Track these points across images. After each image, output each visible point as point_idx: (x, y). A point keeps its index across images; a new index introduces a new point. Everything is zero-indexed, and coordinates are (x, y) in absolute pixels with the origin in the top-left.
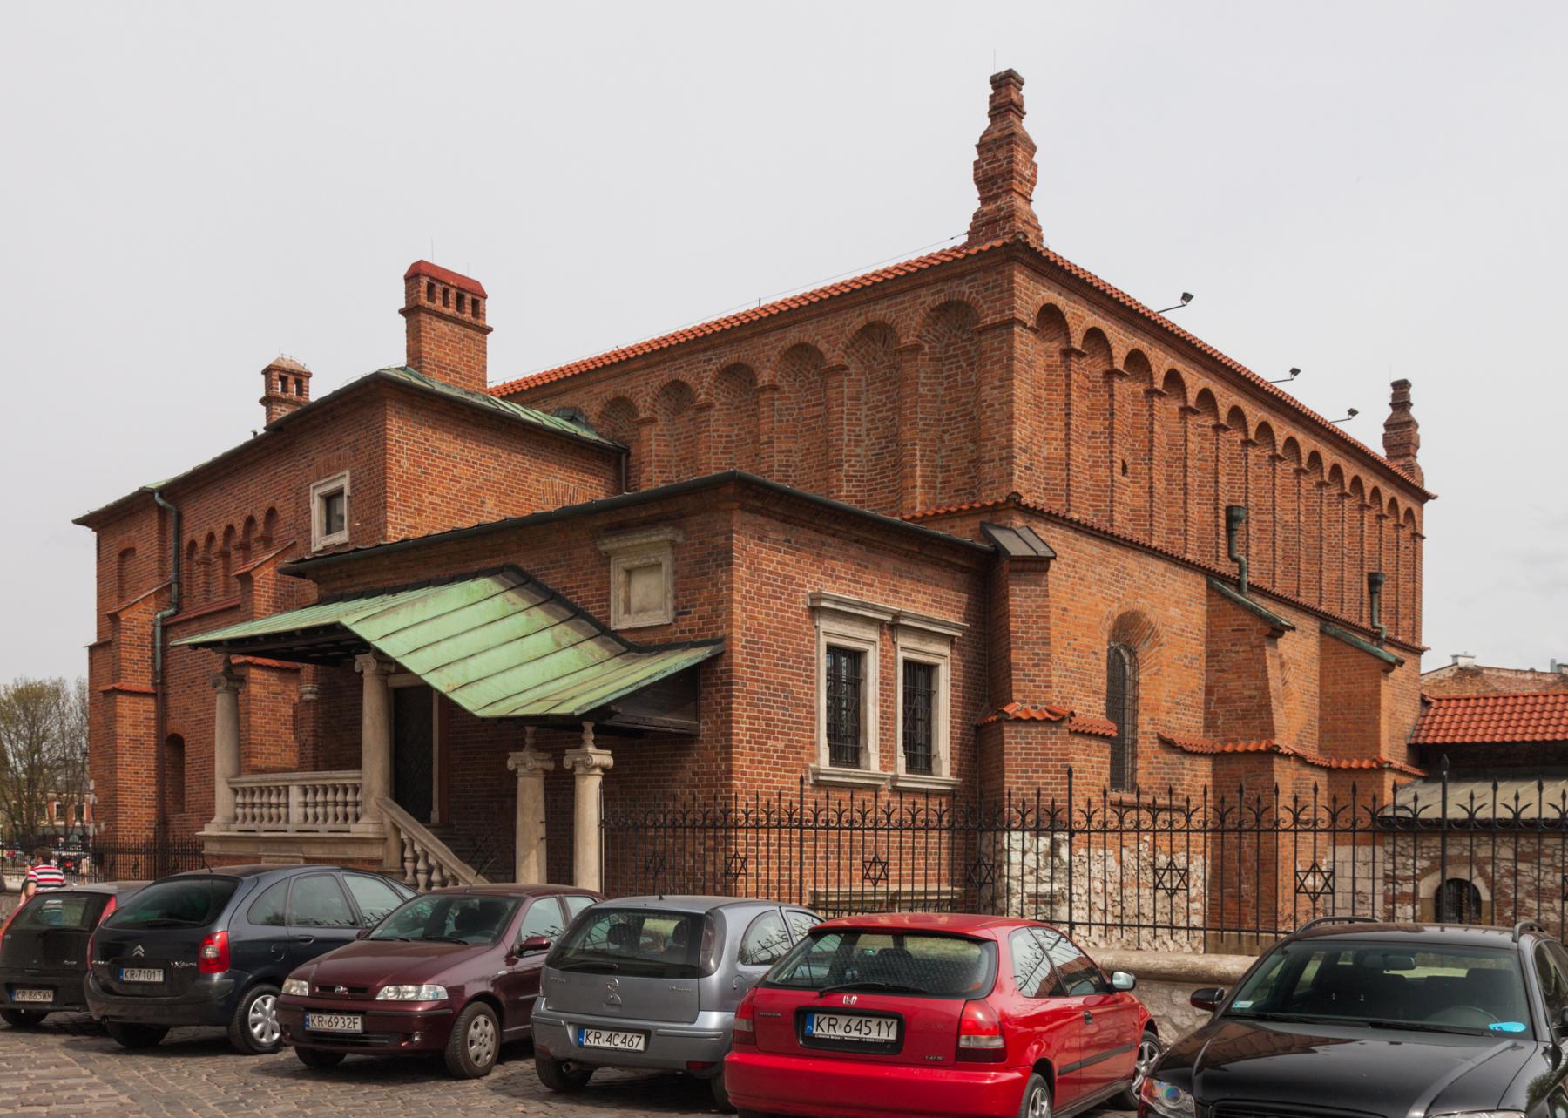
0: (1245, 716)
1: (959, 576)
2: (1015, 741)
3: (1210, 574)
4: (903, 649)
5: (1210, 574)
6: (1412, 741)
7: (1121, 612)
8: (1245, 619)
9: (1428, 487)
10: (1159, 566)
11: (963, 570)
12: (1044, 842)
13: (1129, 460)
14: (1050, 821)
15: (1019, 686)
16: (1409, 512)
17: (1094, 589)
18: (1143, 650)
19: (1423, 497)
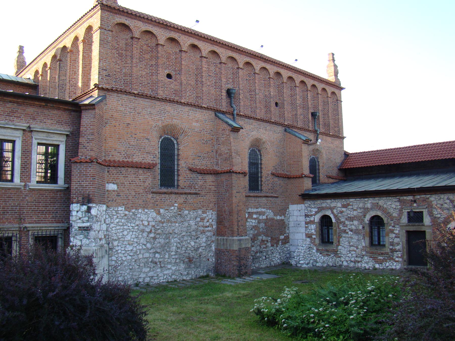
0: (226, 159)
1: (73, 113)
2: (76, 170)
3: (217, 111)
4: (36, 139)
5: (217, 111)
6: (338, 168)
7: (164, 124)
8: (225, 126)
9: (342, 86)
10: (187, 109)
11: (74, 111)
12: (85, 208)
13: (173, 73)
14: (87, 200)
15: (81, 150)
16: (333, 93)
17: (147, 117)
18: (181, 138)
19: (342, 89)
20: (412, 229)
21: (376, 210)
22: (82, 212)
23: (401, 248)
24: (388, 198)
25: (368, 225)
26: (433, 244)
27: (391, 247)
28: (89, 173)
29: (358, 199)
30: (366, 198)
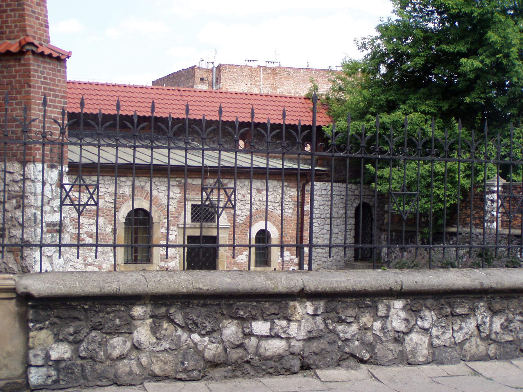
20: (196, 233)
21: (140, 200)
22: (51, 185)
23: (178, 265)
24: (161, 179)
25: (124, 226)
26: (228, 257)
27: (162, 264)
28: (57, 86)
29: (109, 178)
30: (123, 176)
